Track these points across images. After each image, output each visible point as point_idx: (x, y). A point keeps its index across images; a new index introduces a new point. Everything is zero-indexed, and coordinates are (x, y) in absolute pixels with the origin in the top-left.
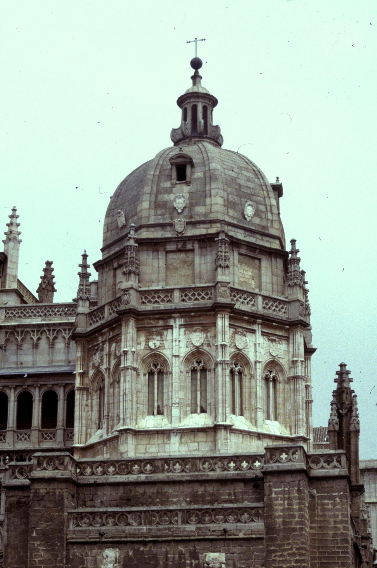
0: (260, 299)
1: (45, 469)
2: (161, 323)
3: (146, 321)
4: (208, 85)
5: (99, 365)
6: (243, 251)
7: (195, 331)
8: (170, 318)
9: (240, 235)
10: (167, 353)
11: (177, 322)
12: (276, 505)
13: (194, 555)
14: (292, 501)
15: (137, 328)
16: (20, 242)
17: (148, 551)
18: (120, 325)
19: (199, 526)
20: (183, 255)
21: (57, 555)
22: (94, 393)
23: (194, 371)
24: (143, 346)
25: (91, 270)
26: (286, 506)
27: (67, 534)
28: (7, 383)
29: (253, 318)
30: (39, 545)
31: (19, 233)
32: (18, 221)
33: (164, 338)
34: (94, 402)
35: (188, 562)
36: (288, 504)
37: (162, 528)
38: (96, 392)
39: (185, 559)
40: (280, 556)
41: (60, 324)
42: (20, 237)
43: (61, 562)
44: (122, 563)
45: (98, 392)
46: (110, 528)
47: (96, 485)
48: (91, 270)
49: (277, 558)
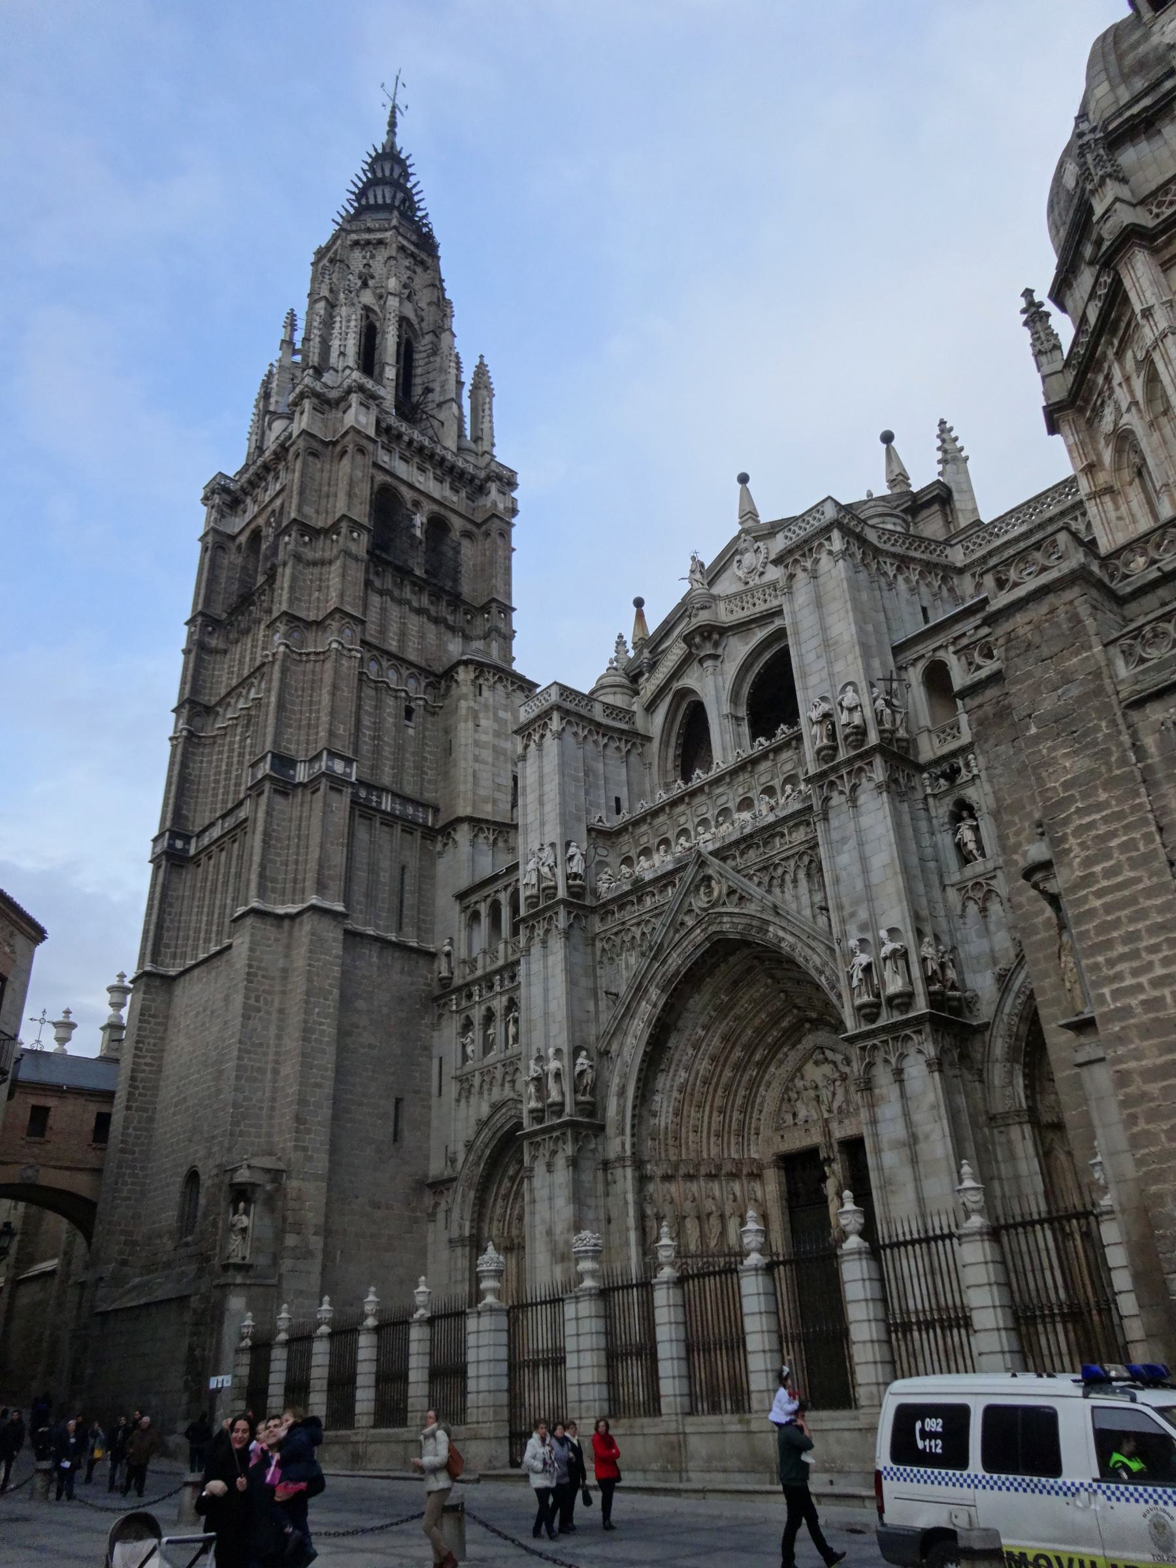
1: (1016, 585)
5: (1116, 424)
15: (1162, 265)
16: (967, 458)
18: (1126, 299)
21: (1107, 752)
22: (1128, 489)
25: (1049, 307)
27: (1118, 693)
30: (1052, 749)
31: (962, 449)
32: (953, 434)
34: (1134, 504)
38: (1131, 484)
41: (1062, 514)
42: (964, 454)
45: (1137, 480)
48: (1049, 307)
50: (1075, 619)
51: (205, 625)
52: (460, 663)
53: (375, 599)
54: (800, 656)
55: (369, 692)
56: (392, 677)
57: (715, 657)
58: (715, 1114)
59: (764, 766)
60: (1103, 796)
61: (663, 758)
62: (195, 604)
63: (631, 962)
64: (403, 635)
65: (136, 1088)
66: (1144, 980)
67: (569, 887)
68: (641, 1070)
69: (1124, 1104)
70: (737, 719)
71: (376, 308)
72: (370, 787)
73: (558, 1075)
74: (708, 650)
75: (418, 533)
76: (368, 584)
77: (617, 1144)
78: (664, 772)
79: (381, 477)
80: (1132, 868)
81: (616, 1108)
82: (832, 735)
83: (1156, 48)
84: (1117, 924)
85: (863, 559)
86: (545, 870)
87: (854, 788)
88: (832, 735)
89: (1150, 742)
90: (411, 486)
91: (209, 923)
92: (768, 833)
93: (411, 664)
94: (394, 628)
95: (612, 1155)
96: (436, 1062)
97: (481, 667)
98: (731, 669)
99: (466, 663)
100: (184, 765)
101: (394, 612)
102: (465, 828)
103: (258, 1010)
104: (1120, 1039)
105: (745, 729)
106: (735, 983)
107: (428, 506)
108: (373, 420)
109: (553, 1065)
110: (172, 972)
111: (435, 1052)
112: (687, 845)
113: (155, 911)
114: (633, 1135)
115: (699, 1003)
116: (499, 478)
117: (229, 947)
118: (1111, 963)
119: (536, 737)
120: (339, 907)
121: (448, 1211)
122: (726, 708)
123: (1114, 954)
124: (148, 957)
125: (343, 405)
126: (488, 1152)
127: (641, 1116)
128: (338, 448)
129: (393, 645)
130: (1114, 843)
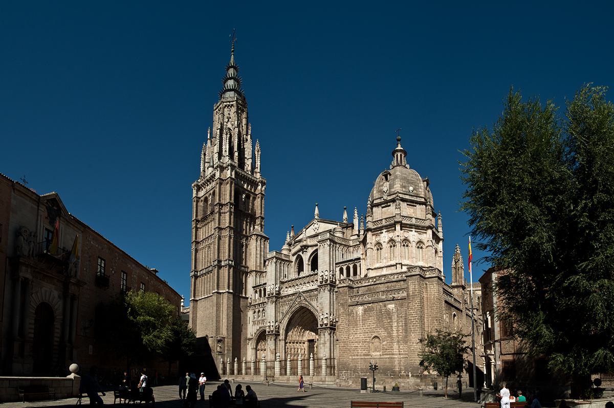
13: (385, 306)
37: (375, 298)
46: (360, 300)
47: (359, 287)
50: (346, 291)
57: (306, 252)
61: (295, 266)
63: (286, 308)
73: (273, 326)
74: (305, 250)
77: (282, 337)
78: (295, 269)
81: (282, 332)
82: (323, 279)
86: (271, 289)
88: (323, 279)
92: (311, 290)
98: (309, 254)
105: (310, 267)
109: (272, 324)
122: (307, 263)
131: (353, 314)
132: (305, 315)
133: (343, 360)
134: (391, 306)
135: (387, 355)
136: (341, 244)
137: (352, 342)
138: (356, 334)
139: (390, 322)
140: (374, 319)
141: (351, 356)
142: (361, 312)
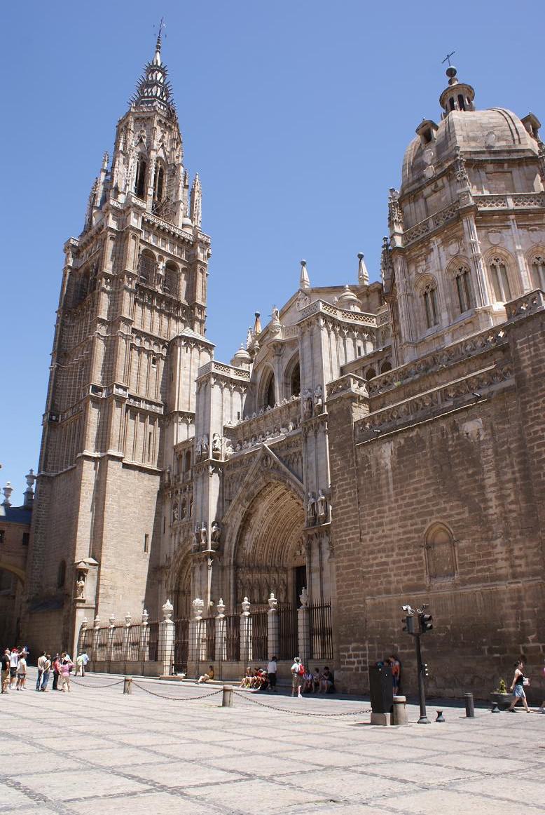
0: (510, 201)
2: (424, 250)
3: (413, 254)
4: (460, 79)
6: (490, 167)
7: (452, 243)
8: (429, 243)
9: (483, 157)
10: (431, 271)
11: (436, 242)
12: (523, 355)
13: (455, 428)
14: (537, 345)
17: (416, 436)
19: (456, 399)
20: (438, 194)
23: (458, 278)
24: (414, 273)
26: (533, 353)
28: (373, 360)
29: (505, 214)
33: (428, 260)
35: (450, 436)
36: (535, 351)
39: (447, 435)
40: (535, 405)
43: (353, 465)
44: (396, 453)
49: (533, 409)
51: (64, 314)
52: (177, 337)
53: (139, 308)
54: (303, 369)
55: (135, 352)
56: (147, 346)
58: (270, 549)
59: (294, 408)
60: (346, 476)
62: (60, 303)
64: (152, 323)
65: (39, 524)
66: (347, 538)
67: (213, 454)
68: (238, 533)
69: (337, 576)
70: (287, 384)
71: (146, 153)
72: (136, 399)
75: (161, 272)
76: (136, 301)
78: (260, 401)
79: (143, 247)
80: (350, 502)
83: (423, 161)
84: (343, 519)
85: (333, 327)
87: (316, 432)
88: (311, 407)
89: (359, 459)
90: (158, 250)
91: (67, 455)
93: (155, 338)
94: (148, 319)
95: (225, 564)
96: (163, 519)
97: (189, 340)
99: (181, 338)
100: (56, 381)
101: (148, 312)
102: (178, 415)
103: (87, 498)
104: (339, 556)
106: (278, 499)
107: (166, 259)
108: (140, 219)
110: (53, 475)
111: (163, 514)
112: (262, 439)
113: (45, 448)
114: (234, 557)
115: (263, 506)
116: (201, 241)
117: (75, 468)
118: (341, 531)
119: (204, 385)
120: (120, 455)
121: (167, 581)
122: (282, 378)
123: (341, 529)
124: (42, 469)
125: (126, 214)
126: (182, 558)
127: (238, 549)
128: (124, 235)
129: (147, 330)
130: (347, 492)
131: (369, 467)
132: (282, 503)
133: (348, 610)
134: (472, 427)
135: (477, 580)
136: (352, 327)
137: (372, 552)
138: (381, 524)
139: (474, 474)
140: (427, 473)
141: (371, 594)
142: (388, 461)
